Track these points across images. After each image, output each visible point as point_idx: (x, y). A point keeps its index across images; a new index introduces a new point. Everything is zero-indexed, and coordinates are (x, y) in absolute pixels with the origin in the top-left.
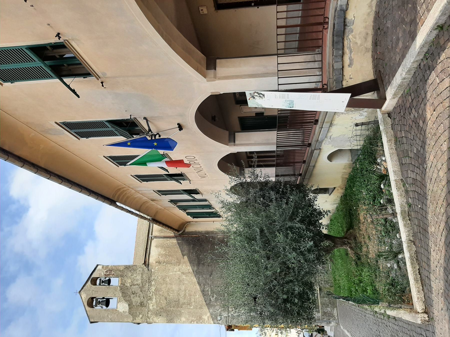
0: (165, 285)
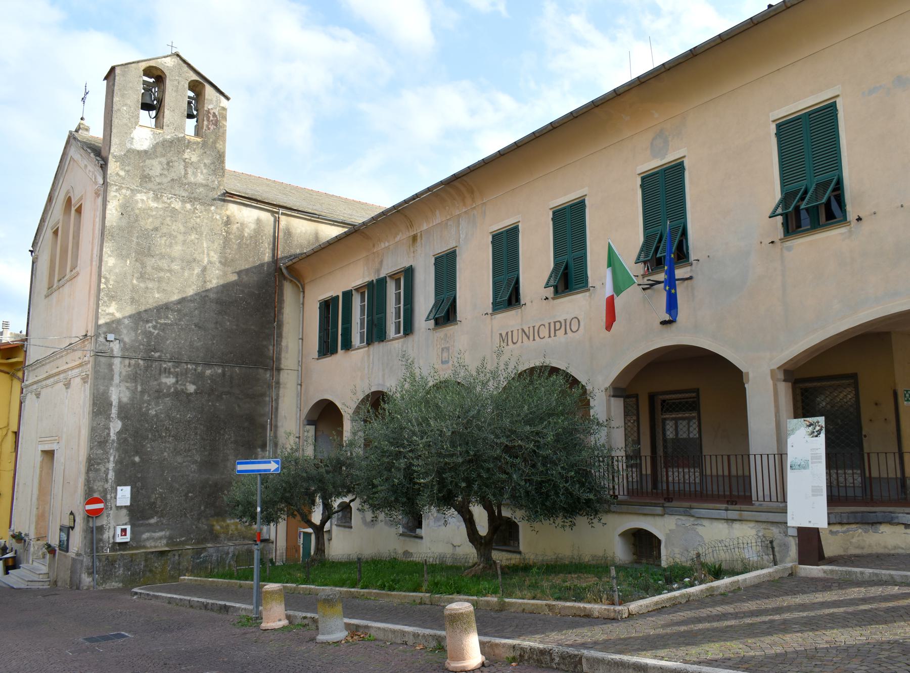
0: (182, 229)
